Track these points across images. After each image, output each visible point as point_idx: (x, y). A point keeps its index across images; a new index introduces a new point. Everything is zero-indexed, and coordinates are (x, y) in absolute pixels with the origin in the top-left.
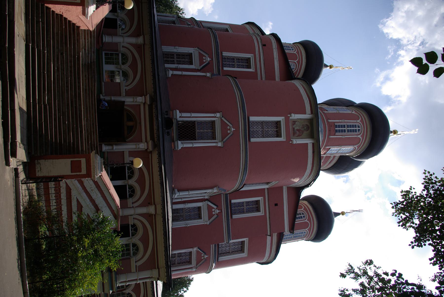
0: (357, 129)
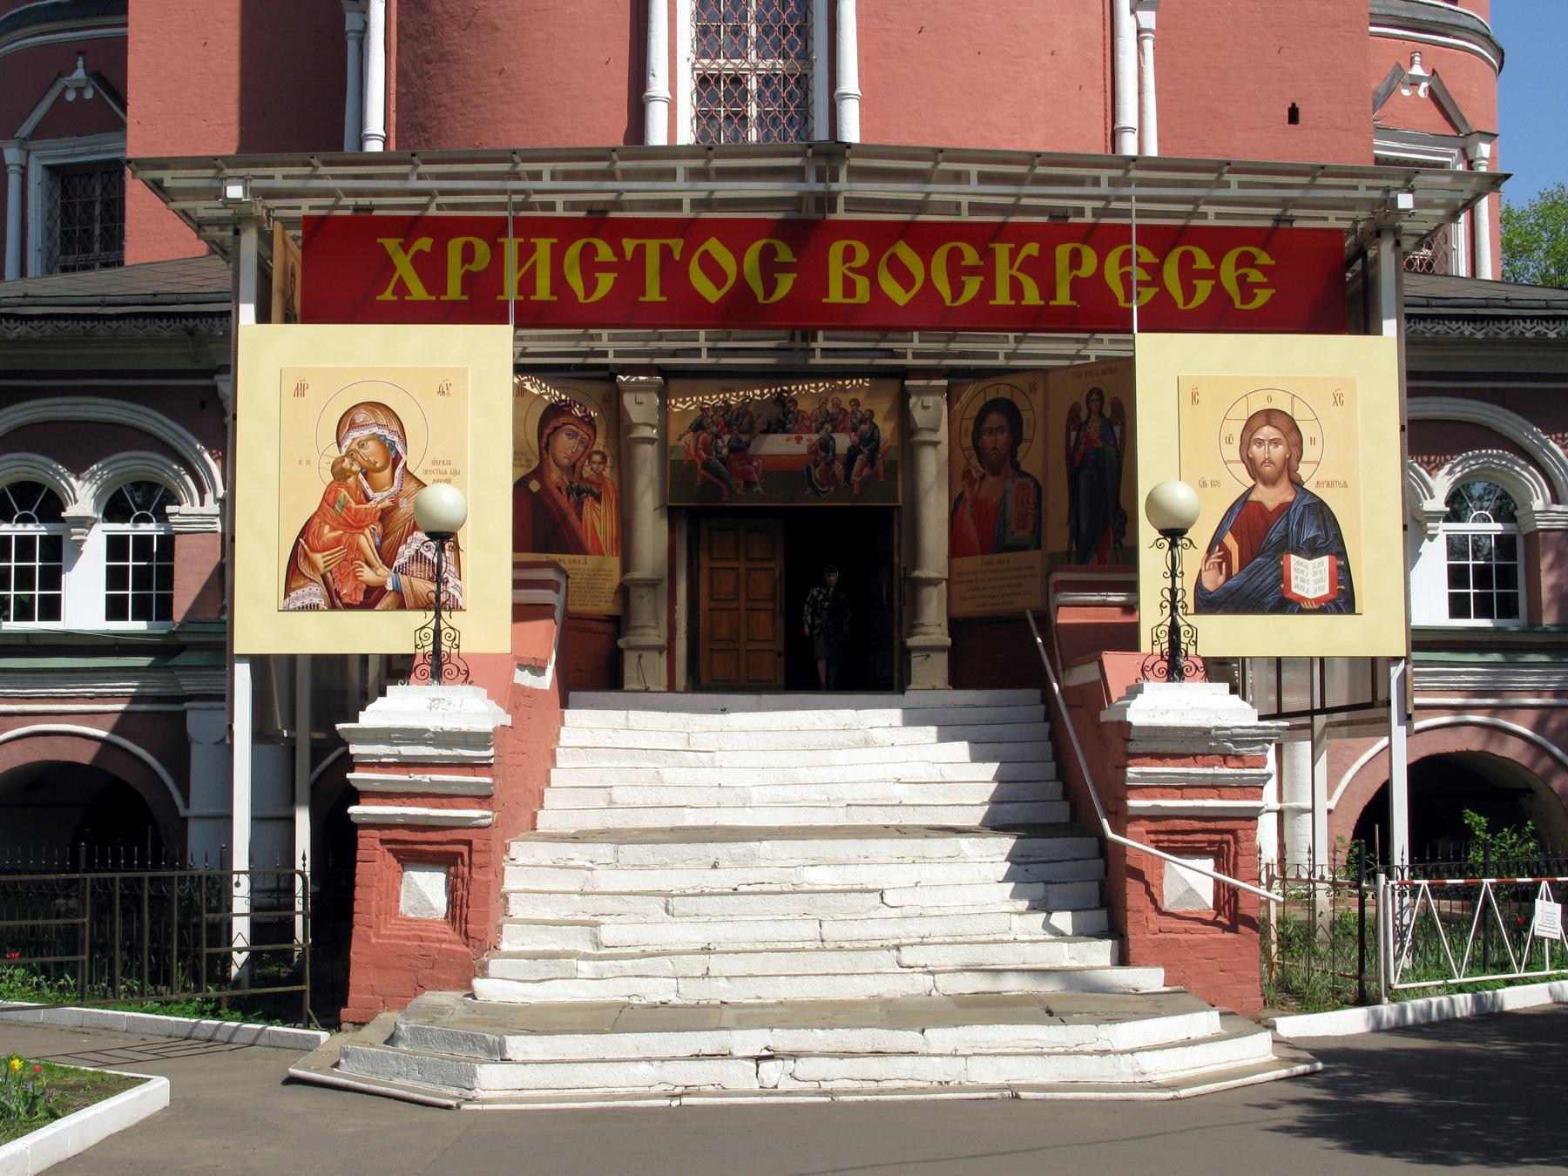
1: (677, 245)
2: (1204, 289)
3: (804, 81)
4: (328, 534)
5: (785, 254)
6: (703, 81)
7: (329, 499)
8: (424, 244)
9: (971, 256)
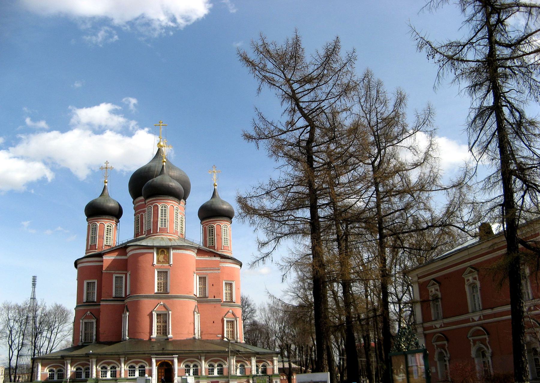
6: (157, 326)
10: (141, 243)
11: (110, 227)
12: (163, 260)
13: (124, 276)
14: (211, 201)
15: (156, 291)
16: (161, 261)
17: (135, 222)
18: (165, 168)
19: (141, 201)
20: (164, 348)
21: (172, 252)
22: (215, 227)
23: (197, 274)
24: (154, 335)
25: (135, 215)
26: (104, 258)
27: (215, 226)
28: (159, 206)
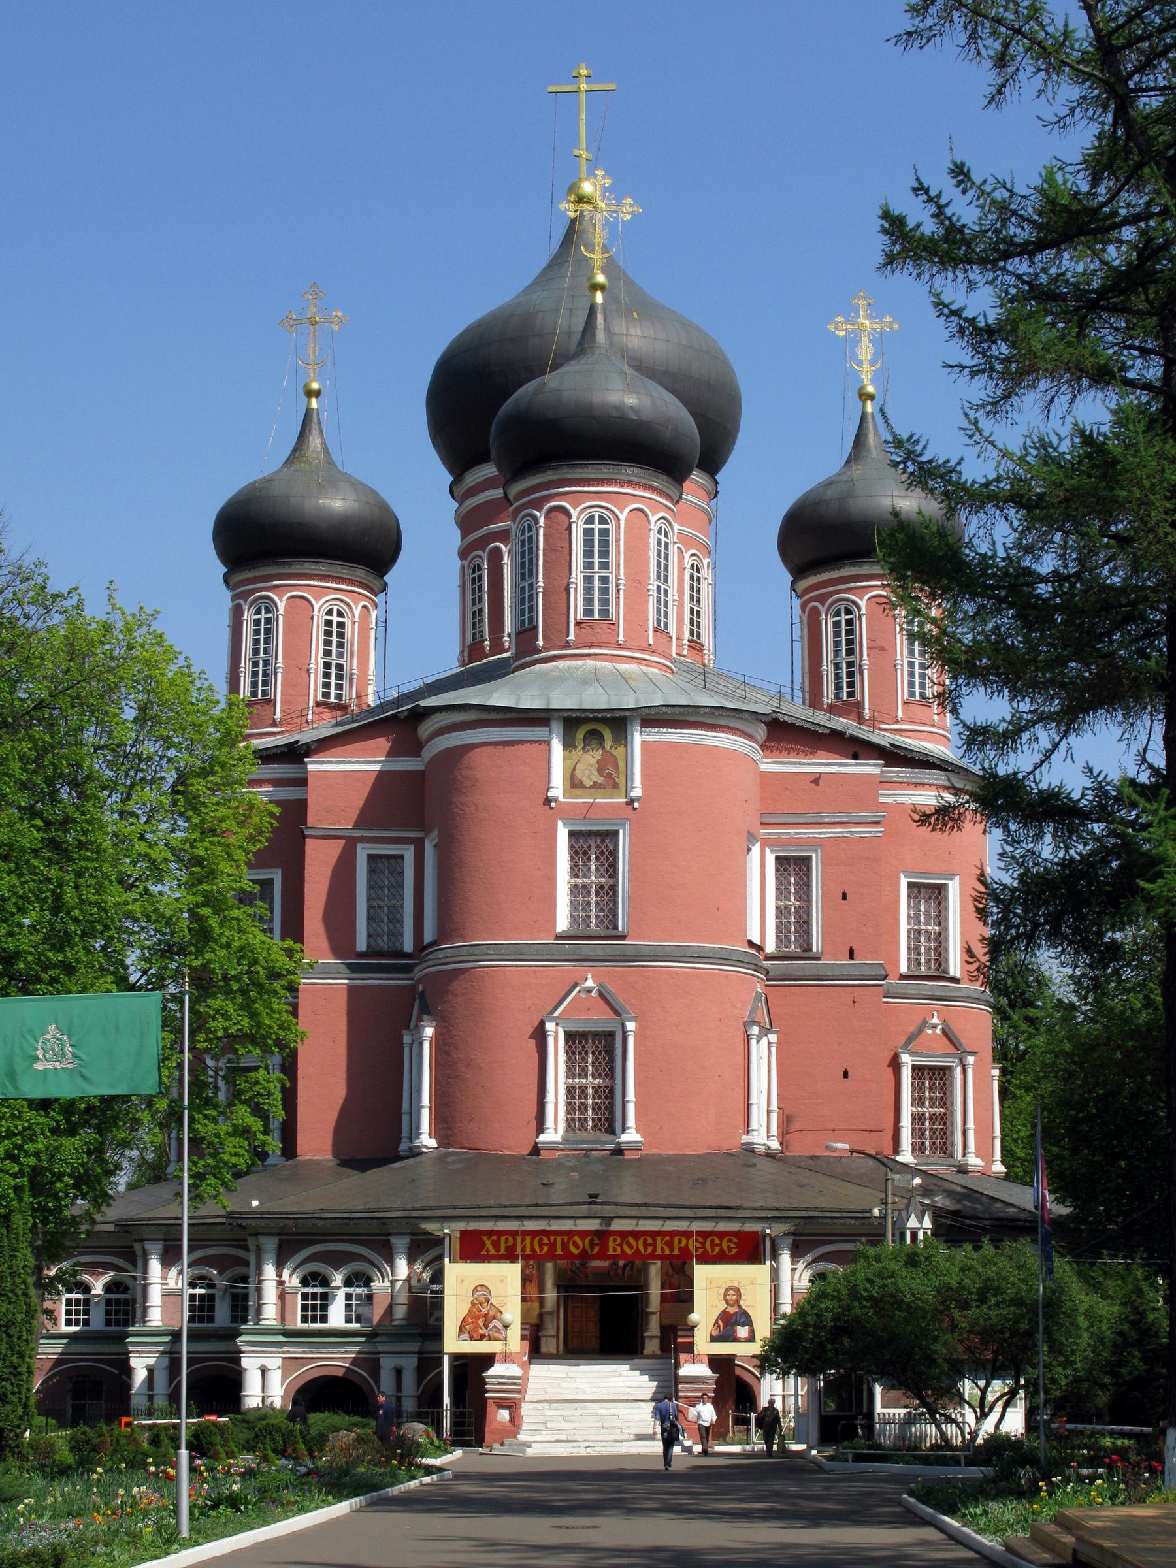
0: (600, 530)
1: (566, 1238)
2: (717, 1249)
3: (611, 1090)
4: (470, 1320)
5: (596, 1241)
7: (470, 1311)
8: (494, 1238)
9: (650, 1240)
10: (490, 694)
11: (340, 614)
12: (600, 780)
13: (409, 853)
14: (845, 477)
15: (562, 923)
16: (588, 783)
17: (463, 587)
18: (600, 319)
19: (487, 484)
20: (595, 1196)
21: (638, 738)
22: (863, 611)
23: (766, 842)
24: (554, 1133)
25: (463, 554)
26: (310, 768)
27: (863, 604)
28: (574, 513)
